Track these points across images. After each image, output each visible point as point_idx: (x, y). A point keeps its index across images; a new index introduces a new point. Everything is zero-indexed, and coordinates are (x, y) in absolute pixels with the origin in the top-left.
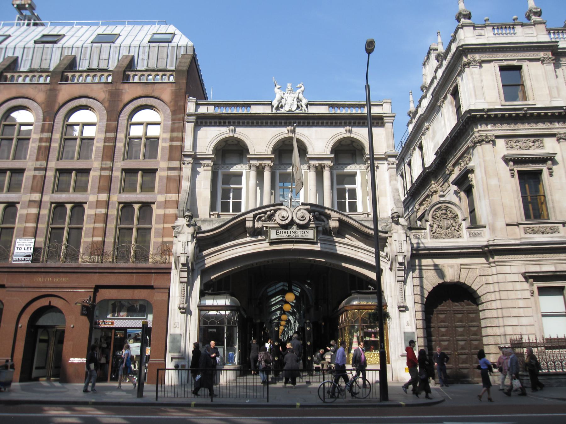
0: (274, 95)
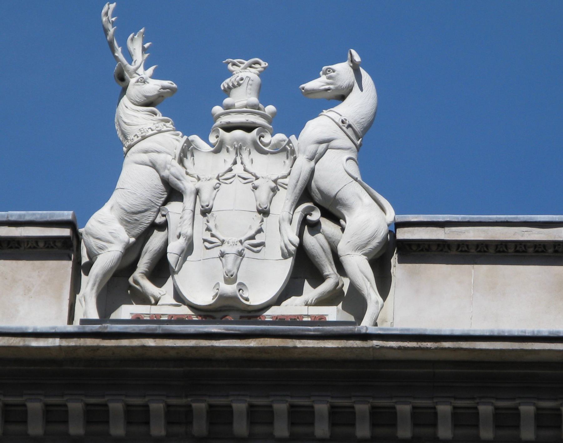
0: (111, 152)
